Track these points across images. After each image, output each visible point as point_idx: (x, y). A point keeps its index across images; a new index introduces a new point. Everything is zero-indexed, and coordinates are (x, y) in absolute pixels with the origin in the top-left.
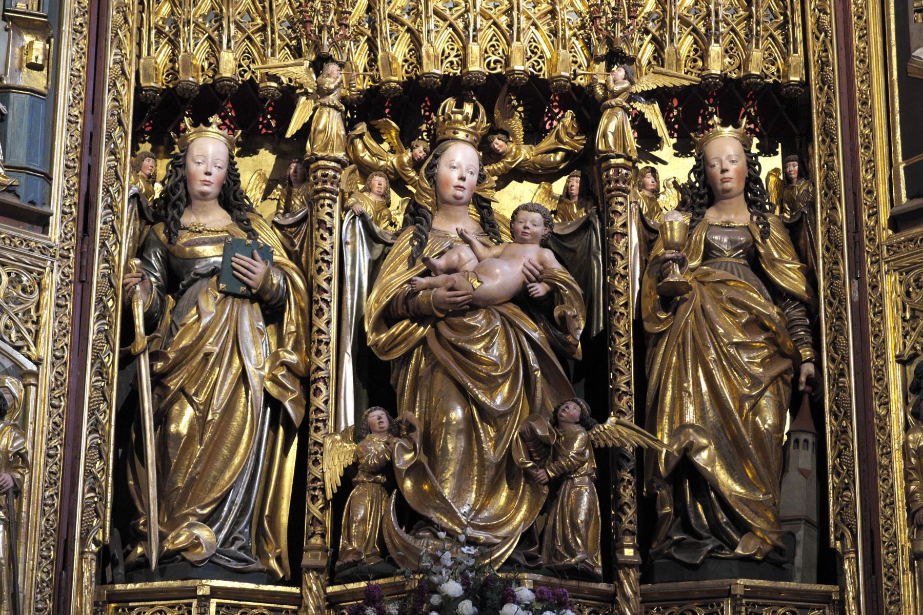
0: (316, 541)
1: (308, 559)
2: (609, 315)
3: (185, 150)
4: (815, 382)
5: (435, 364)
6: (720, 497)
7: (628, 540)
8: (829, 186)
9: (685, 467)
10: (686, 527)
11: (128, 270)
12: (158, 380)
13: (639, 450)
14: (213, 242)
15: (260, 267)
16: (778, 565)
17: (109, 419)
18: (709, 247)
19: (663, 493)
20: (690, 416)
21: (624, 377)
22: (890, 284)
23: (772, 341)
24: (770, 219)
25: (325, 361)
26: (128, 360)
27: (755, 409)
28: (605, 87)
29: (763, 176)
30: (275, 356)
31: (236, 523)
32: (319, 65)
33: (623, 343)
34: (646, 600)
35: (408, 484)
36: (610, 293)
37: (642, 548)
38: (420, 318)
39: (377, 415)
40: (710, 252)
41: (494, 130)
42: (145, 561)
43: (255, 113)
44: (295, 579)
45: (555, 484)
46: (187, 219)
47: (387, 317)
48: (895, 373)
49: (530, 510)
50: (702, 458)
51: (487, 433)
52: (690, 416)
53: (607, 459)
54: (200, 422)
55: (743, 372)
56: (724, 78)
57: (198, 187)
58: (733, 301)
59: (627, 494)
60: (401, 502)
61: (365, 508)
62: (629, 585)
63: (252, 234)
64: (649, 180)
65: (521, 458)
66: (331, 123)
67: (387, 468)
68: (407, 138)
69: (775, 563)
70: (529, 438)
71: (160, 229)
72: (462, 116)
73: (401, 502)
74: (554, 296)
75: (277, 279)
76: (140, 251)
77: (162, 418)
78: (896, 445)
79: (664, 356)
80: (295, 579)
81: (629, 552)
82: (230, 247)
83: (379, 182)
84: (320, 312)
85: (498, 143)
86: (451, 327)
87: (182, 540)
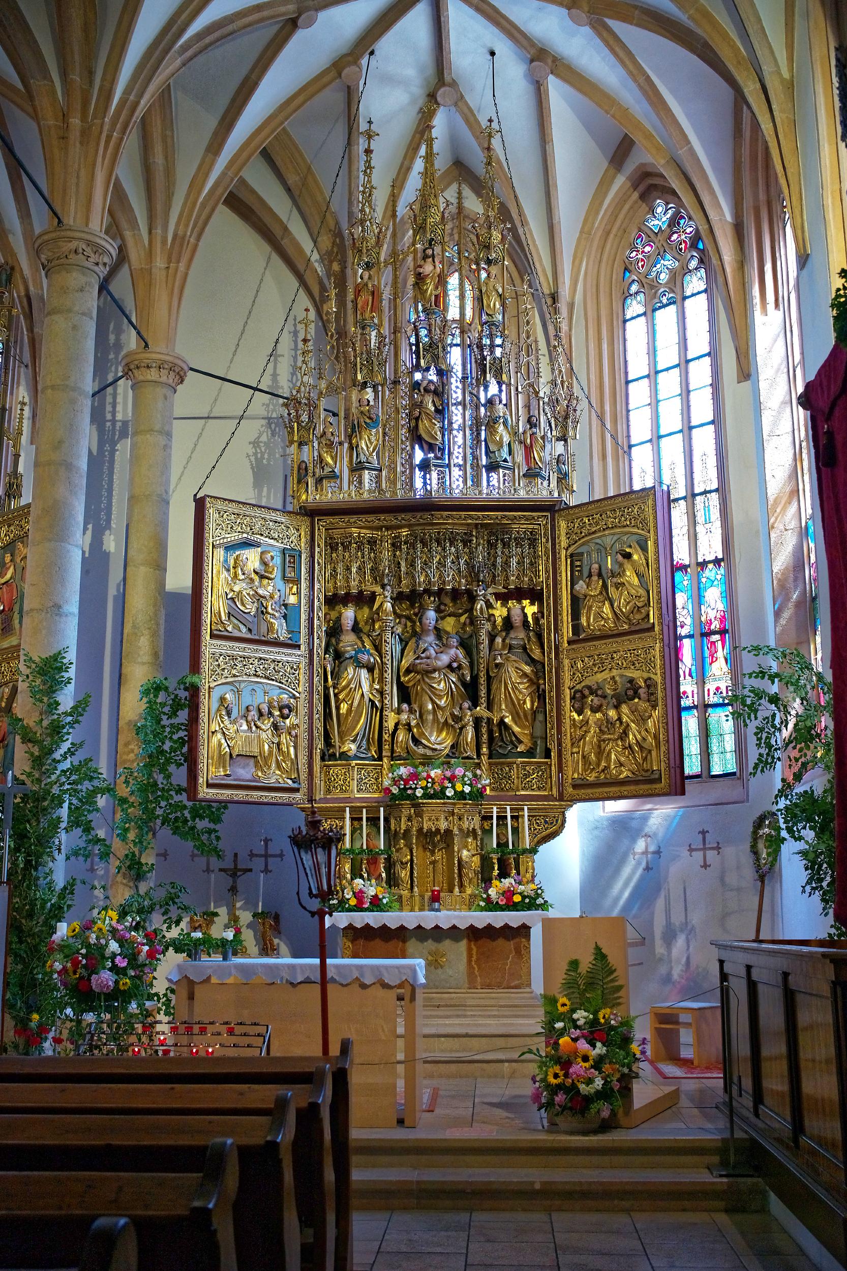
0: (387, 747)
1: (384, 754)
2: (478, 670)
3: (341, 614)
4: (544, 691)
5: (423, 689)
6: (513, 733)
7: (484, 745)
8: (549, 622)
9: (502, 722)
10: (502, 740)
11: (325, 659)
12: (336, 695)
13: (488, 719)
14: (352, 645)
15: (366, 657)
16: (532, 753)
17: (320, 708)
18: (510, 646)
19: (495, 729)
20: (503, 707)
21: (483, 692)
22: (566, 662)
23: (530, 680)
24: (531, 634)
25: (387, 688)
26: (326, 689)
27: (525, 702)
28: (476, 591)
29: (530, 619)
30: (371, 686)
31: (362, 740)
32: (383, 587)
33: (482, 680)
34: (490, 764)
35: (415, 730)
36: (479, 664)
37: (489, 748)
38: (418, 672)
39: (405, 706)
40: (511, 647)
41: (441, 603)
42: (335, 755)
43: (364, 599)
44: (381, 760)
45: (461, 729)
46: (343, 637)
47: (408, 671)
48: (568, 691)
49: (454, 738)
50: (506, 720)
51: (440, 714)
52: (503, 707)
53: (477, 721)
54: (349, 710)
55: (521, 692)
56: (516, 588)
57: (345, 628)
58: (517, 668)
59: (484, 730)
60: (413, 737)
61: (401, 736)
62: (484, 759)
63: (363, 642)
64: (492, 618)
65: (450, 721)
66: (388, 606)
67: (409, 724)
68: (412, 606)
69: (530, 753)
70: (452, 714)
71: (333, 641)
72: (430, 603)
73: (413, 737)
74: (460, 667)
75: (372, 660)
76: (327, 651)
77: (338, 708)
78: (568, 715)
79: (494, 687)
80: (380, 758)
81: (485, 750)
82: (357, 653)
83: (403, 620)
84: (386, 671)
85: (442, 607)
86: (428, 677)
87: (345, 749)
